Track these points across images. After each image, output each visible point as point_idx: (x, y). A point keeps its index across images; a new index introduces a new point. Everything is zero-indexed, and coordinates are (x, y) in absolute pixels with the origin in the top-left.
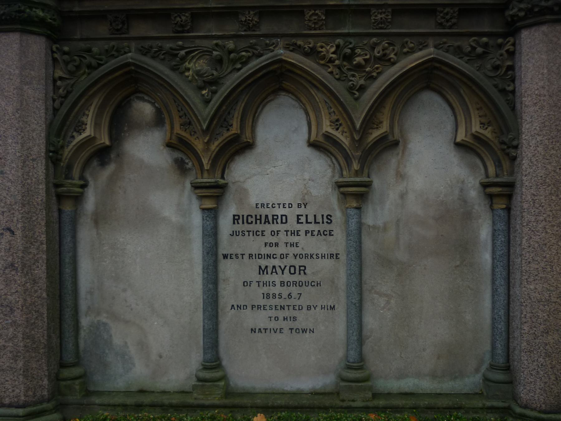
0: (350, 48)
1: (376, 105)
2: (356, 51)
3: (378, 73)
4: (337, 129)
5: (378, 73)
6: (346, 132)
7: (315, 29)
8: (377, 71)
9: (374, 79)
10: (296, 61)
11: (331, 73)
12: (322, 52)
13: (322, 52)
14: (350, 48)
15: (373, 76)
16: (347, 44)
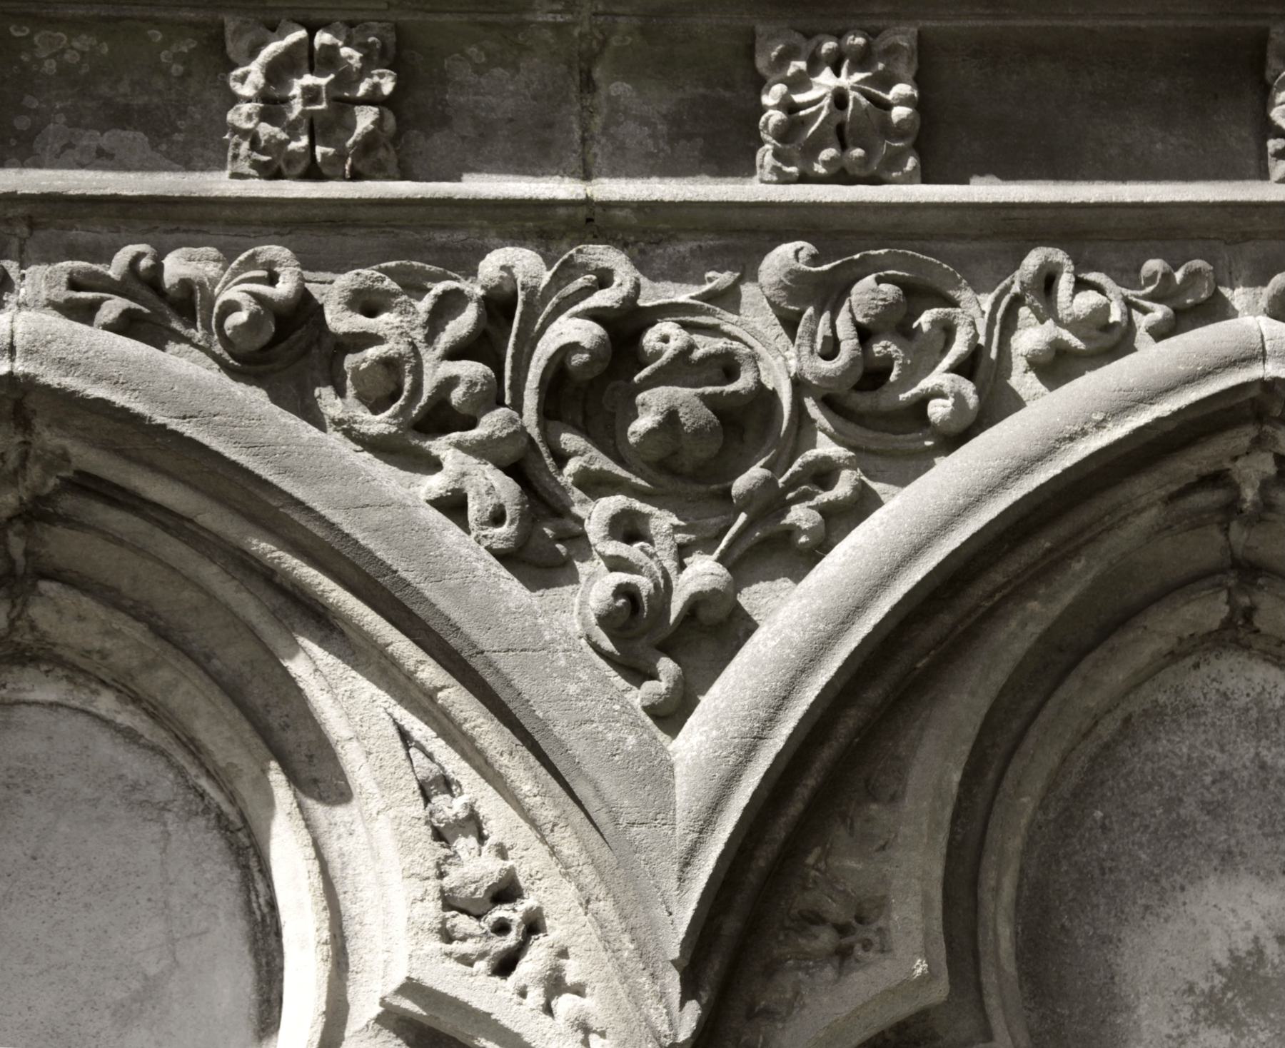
0: (595, 315)
1: (827, 754)
2: (650, 340)
3: (827, 511)
4: (505, 965)
5: (827, 511)
6: (579, 990)
7: (313, 173)
8: (824, 497)
9: (796, 557)
10: (152, 399)
11: (453, 505)
12: (375, 339)
13: (375, 339)
14: (595, 315)
15: (792, 531)
16: (580, 282)
